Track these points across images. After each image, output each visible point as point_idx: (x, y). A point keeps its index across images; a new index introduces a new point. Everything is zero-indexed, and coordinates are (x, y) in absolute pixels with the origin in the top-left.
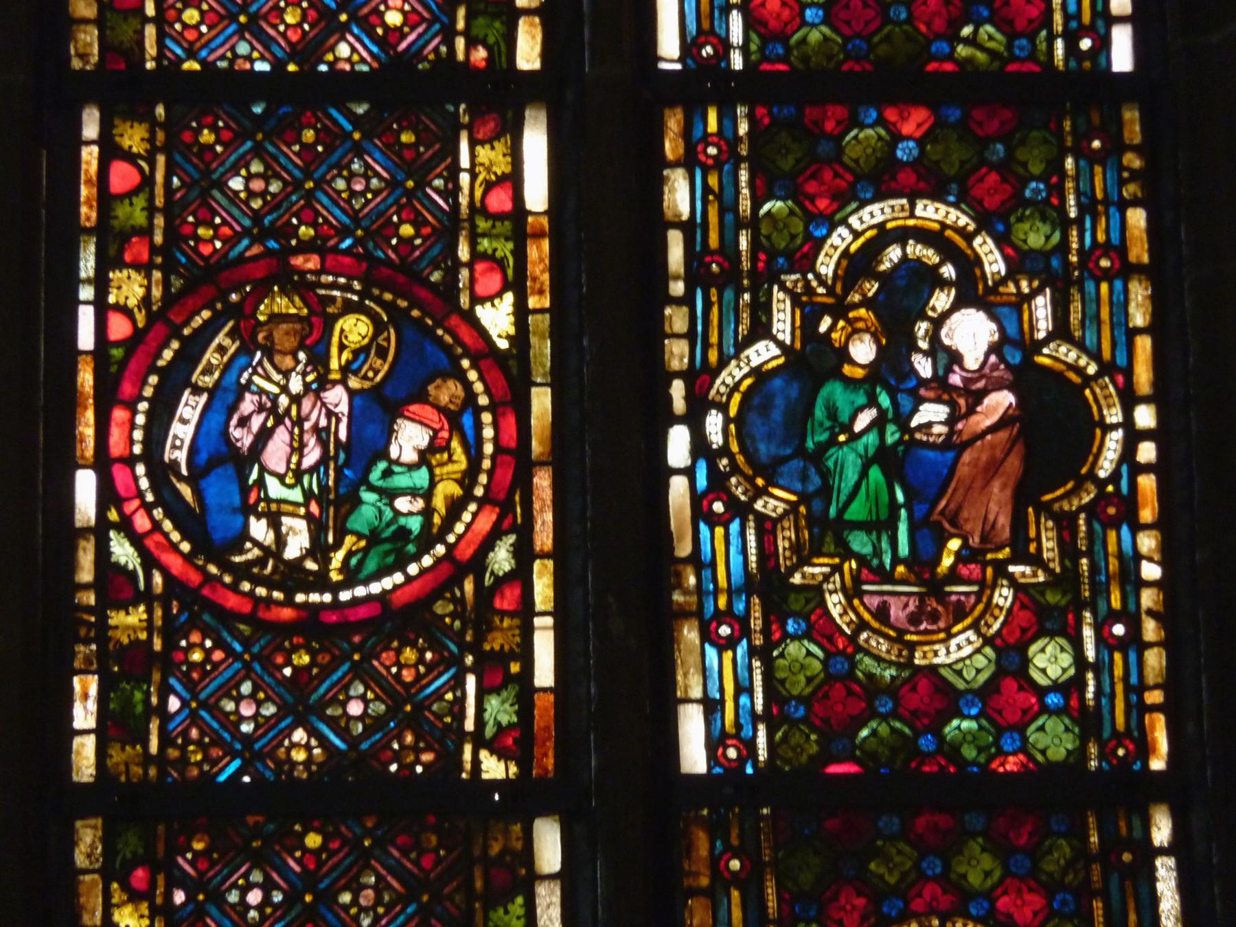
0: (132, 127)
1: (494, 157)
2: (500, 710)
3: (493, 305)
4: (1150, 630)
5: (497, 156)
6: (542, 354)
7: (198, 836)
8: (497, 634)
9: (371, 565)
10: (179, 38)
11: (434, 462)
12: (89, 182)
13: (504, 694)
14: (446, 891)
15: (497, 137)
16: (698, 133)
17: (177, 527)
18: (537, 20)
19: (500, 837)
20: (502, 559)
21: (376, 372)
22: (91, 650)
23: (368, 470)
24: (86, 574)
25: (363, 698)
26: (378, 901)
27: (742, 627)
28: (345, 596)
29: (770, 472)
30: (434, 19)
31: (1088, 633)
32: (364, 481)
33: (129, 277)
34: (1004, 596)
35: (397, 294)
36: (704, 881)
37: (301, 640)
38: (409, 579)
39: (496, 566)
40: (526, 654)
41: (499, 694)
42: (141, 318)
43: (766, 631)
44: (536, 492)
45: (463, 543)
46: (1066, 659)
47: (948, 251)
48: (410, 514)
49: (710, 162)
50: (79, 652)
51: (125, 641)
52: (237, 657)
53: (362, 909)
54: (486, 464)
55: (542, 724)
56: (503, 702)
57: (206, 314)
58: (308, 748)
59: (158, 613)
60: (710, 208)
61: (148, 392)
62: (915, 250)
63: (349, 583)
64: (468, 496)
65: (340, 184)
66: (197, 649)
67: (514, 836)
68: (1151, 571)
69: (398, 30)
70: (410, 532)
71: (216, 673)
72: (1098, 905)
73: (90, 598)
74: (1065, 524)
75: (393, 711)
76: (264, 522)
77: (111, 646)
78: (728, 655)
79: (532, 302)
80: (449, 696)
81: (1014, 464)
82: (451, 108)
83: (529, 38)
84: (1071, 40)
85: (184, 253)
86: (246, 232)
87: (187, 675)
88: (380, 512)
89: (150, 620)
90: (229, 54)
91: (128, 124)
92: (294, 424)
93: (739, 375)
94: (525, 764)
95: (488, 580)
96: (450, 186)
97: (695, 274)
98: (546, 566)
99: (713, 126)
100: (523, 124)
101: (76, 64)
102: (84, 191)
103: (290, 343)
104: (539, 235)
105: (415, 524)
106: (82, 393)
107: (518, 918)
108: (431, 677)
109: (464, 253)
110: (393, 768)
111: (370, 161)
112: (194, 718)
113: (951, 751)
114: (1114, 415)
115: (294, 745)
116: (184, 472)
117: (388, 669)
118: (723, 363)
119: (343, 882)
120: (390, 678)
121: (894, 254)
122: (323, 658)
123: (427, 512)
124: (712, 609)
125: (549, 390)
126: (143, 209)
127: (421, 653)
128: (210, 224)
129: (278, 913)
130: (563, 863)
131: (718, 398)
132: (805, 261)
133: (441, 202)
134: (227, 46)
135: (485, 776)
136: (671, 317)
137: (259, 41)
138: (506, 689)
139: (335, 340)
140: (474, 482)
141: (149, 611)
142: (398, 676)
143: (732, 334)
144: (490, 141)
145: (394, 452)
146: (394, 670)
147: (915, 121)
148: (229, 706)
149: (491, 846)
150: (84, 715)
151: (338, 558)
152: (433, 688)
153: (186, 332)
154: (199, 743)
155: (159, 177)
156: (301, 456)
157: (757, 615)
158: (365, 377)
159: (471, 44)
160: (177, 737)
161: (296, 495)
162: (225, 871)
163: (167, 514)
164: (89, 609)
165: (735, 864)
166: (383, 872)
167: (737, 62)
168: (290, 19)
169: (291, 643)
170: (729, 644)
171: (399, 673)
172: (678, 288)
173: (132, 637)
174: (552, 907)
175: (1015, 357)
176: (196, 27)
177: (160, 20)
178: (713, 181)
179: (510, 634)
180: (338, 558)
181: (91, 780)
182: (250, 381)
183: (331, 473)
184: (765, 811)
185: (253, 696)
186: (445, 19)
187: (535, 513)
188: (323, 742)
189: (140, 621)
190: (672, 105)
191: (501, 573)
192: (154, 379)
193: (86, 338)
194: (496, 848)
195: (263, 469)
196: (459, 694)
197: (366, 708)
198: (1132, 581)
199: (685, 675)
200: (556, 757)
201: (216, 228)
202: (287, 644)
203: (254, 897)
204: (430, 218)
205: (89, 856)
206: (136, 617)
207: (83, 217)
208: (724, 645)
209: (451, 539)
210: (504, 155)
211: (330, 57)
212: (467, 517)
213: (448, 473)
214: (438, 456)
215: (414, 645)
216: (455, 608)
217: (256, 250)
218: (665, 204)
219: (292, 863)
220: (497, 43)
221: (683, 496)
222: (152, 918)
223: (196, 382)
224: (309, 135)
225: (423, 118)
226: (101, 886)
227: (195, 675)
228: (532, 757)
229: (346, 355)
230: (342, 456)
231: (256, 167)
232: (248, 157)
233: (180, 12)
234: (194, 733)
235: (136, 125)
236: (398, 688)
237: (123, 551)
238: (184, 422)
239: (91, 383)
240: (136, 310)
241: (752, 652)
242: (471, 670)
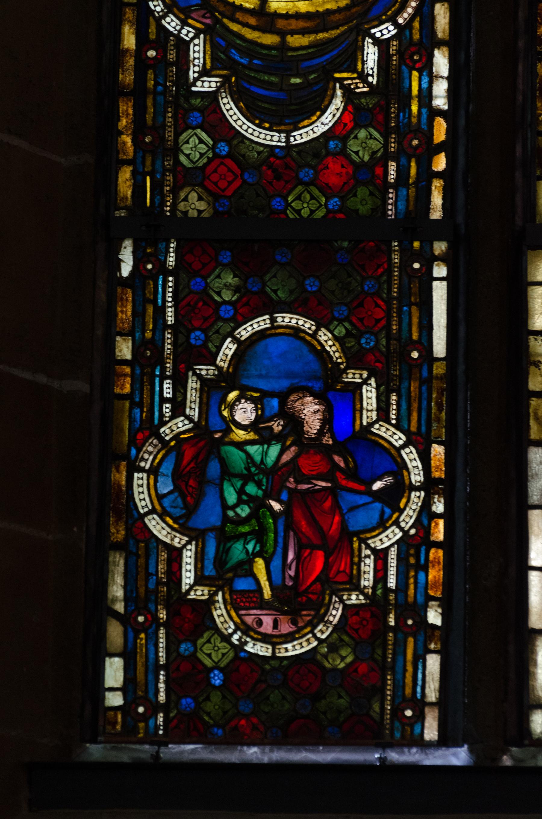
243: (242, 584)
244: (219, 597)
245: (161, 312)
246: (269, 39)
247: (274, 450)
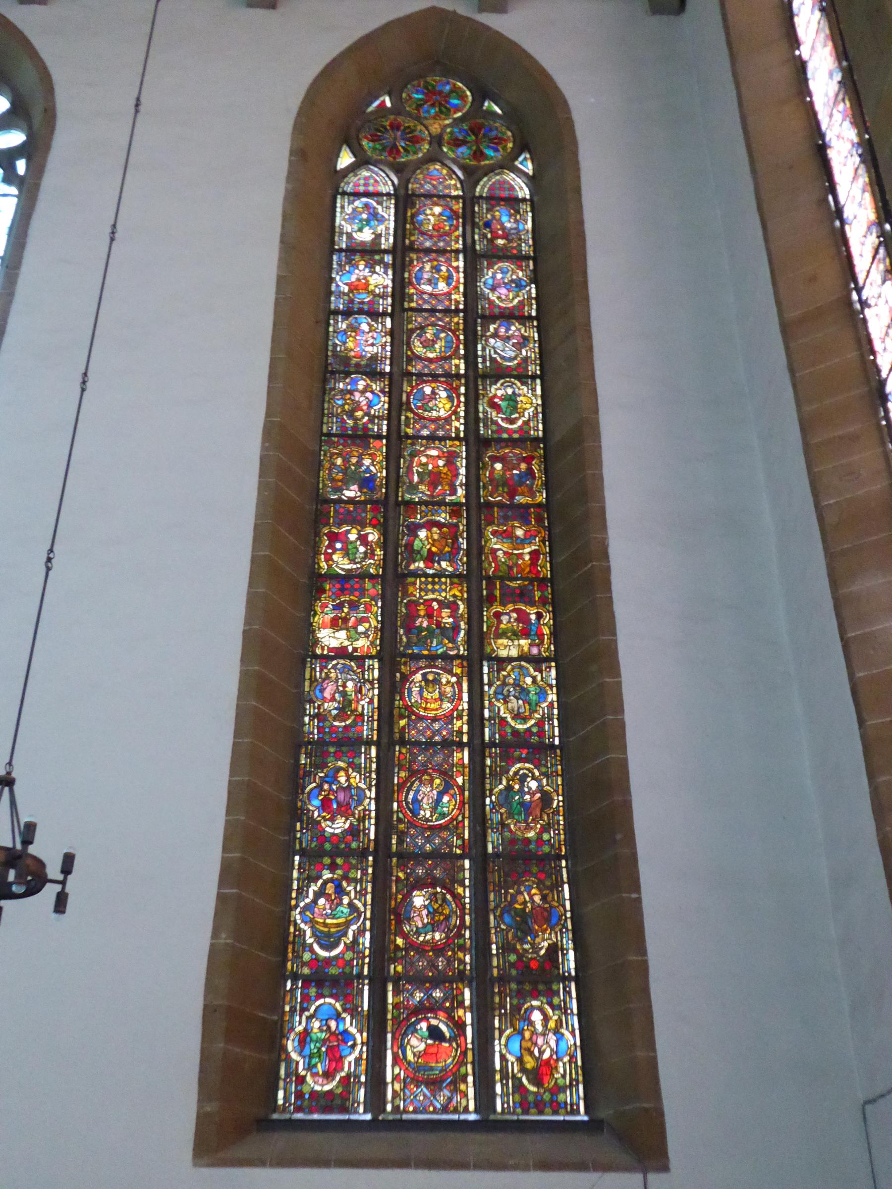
1: (460, 755)
2: (460, 842)
4: (562, 832)
20: (460, 818)
27: (498, 829)
29: (501, 806)
31: (552, 832)
34: (539, 826)
40: (464, 834)
46: (548, 836)
47: (530, 772)
62: (525, 771)
68: (562, 823)
72: (554, 876)
73: (395, 823)
74: (548, 815)
75: (443, 842)
81: (541, 805)
84: (549, 739)
94: (463, 851)
97: (490, 774)
105: (447, 812)
109: (455, 770)
113: (530, 851)
114: (556, 798)
121: (521, 772)
132: (507, 772)
147: (526, 751)
150: (394, 841)
151: (434, 817)
167: (497, 741)
168: (429, 733)
170: (495, 833)
172: (488, 776)
175: (540, 788)
177: (408, 733)
180: (434, 817)
198: (559, 824)
203: (420, 871)
206: (403, 826)
237: (401, 815)
243: (314, 1070)
244: (309, 1074)
245: (296, 998)
246: (326, 930)
247: (324, 1034)
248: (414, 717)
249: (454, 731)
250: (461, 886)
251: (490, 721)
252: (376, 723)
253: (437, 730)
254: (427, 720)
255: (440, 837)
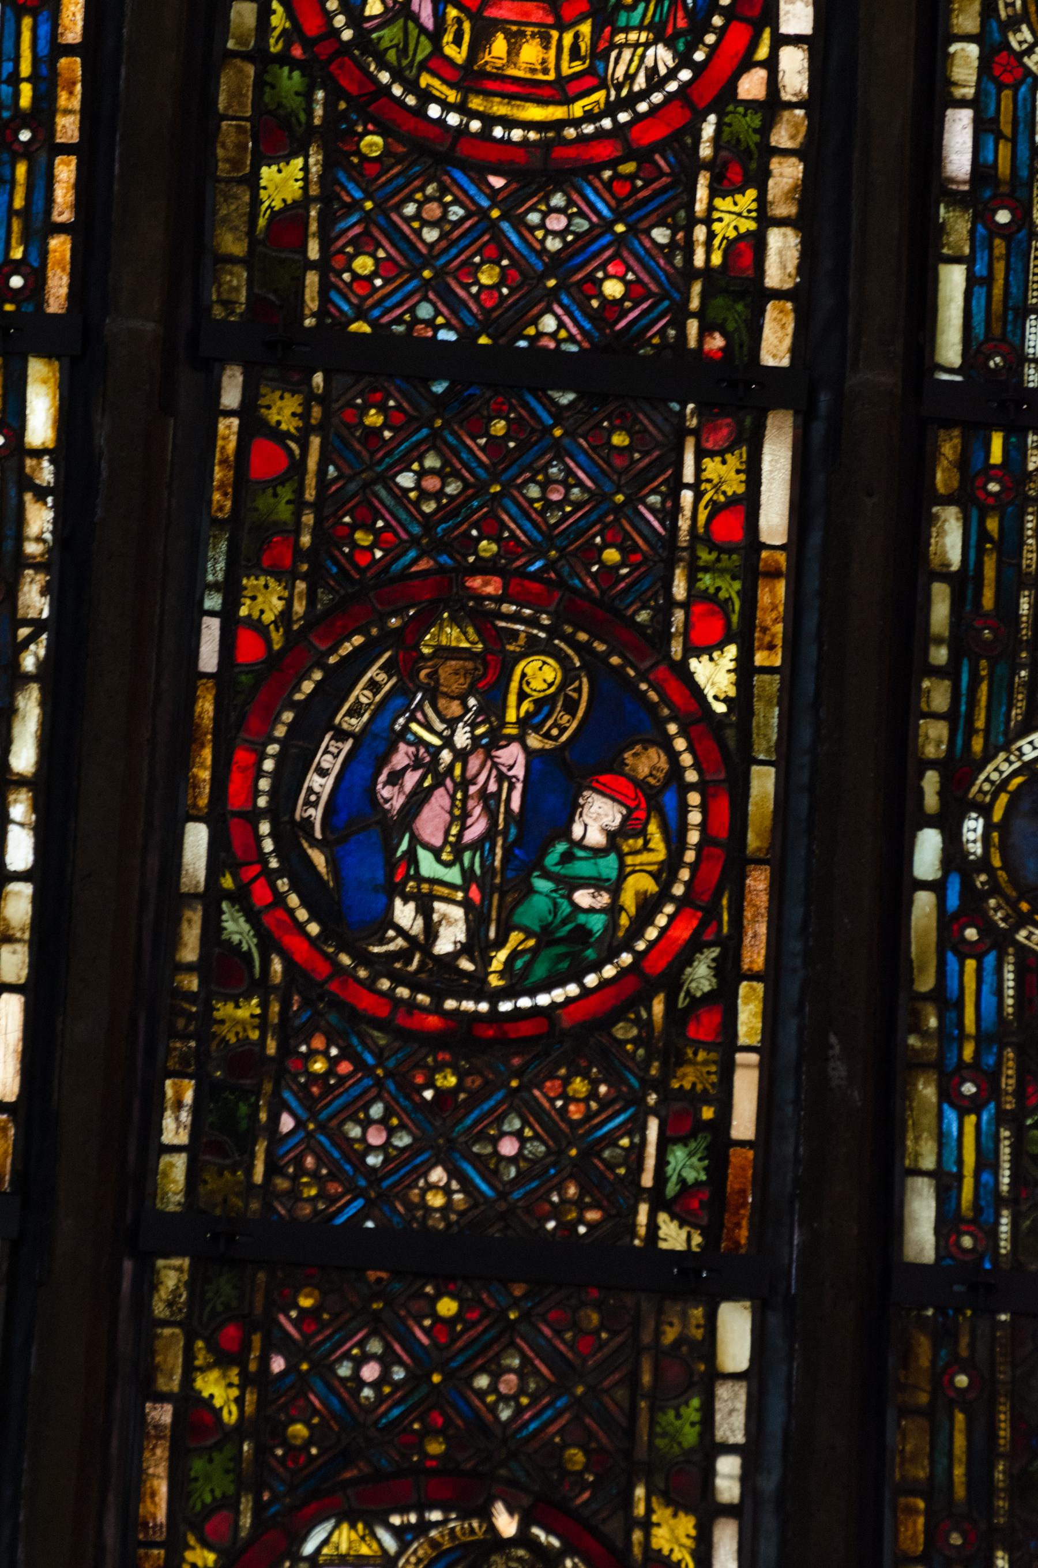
0: (282, 398)
3: (711, 659)
5: (728, 472)
6: (767, 725)
7: (307, 1290)
8: (689, 1069)
9: (540, 971)
10: (346, 290)
11: (626, 849)
12: (224, 462)
13: (693, 1145)
14: (607, 1383)
15: (730, 450)
16: (978, 464)
17: (304, 903)
18: (789, 305)
19: (676, 1321)
21: (563, 730)
22: (190, 1048)
23: (544, 853)
24: (190, 953)
25: (518, 1134)
26: (522, 1391)
28: (505, 1006)
30: (664, 296)
32: (537, 865)
33: (266, 586)
35: (594, 636)
36: (924, 1398)
37: (447, 1057)
38: (585, 991)
39: (694, 985)
41: (686, 1145)
42: (277, 639)
43: (1020, 1093)
44: (748, 897)
45: (654, 953)
48: (591, 910)
49: (991, 501)
50: (175, 1049)
51: (233, 1040)
52: (369, 1071)
53: (503, 1398)
54: (690, 856)
55: (736, 1186)
56: (690, 1155)
57: (358, 640)
58: (447, 1191)
59: (275, 1008)
60: (986, 559)
61: (280, 732)
63: (510, 992)
64: (664, 895)
65: (534, 491)
66: (320, 1057)
67: (694, 1322)
69: (619, 302)
70: (590, 933)
71: (342, 1090)
73: (192, 983)
75: (556, 1154)
76: (412, 905)
77: (214, 1046)
78: (971, 1120)
79: (760, 658)
80: (625, 1142)
82: (675, 406)
83: (778, 328)
85: (336, 563)
86: (415, 541)
87: (305, 1087)
88: (555, 904)
89: (263, 1017)
90: (407, 317)
91: (278, 393)
92: (457, 786)
93: (1007, 769)
94: (711, 1235)
95: (682, 1002)
96: (669, 504)
98: (754, 990)
99: (996, 455)
100: (764, 436)
101: (218, 312)
102: (218, 474)
103: (458, 685)
104: (775, 574)
105: (597, 923)
106: (199, 726)
107: (693, 1424)
108: (603, 1116)
109: (680, 590)
110: (551, 1225)
111: (572, 464)
112: (310, 1144)
115: (431, 1187)
116: (318, 835)
117: (552, 1101)
118: (988, 757)
119: (479, 1362)
120: (553, 1113)
122: (473, 1082)
123: (614, 910)
124: (955, 1060)
125: (772, 770)
126: (288, 502)
127: (594, 1084)
128: (370, 528)
129: (399, 1395)
130: (752, 1360)
131: (980, 798)
133: (656, 524)
134: (405, 307)
135: (663, 1245)
136: (929, 692)
137: (446, 304)
138: (696, 1140)
139: (514, 686)
140: (673, 878)
141: (264, 1005)
142: (563, 1111)
143: (1002, 718)
144: (721, 453)
145: (577, 831)
146: (559, 1103)
148: (355, 1132)
149: (664, 1333)
152: (606, 1129)
153: (332, 660)
154: (315, 1175)
155: (312, 463)
156: (463, 828)
157: (1010, 1072)
158: (547, 736)
159: (704, 331)
160: (287, 1165)
161: (454, 875)
162: (337, 1337)
163: (294, 887)
164: (191, 997)
165: (962, 1380)
166: (531, 1354)
168: (487, 277)
169: (435, 1060)
170: (974, 1105)
171: (565, 1107)
172: (940, 655)
173: (241, 1036)
174: (734, 1414)
176: (369, 278)
177: (323, 266)
178: (992, 525)
179: (705, 1069)
181: (178, 1209)
182: (406, 728)
183: (499, 851)
184: (1003, 1317)
185: (384, 1121)
186: (676, 295)
187: (745, 922)
188: (467, 1185)
189: (252, 1016)
190: (948, 424)
191: (699, 994)
192: (288, 716)
193: (209, 658)
194: (670, 1335)
195: (416, 841)
196: (637, 1140)
197: (522, 1148)
199: (917, 1139)
200: (750, 1230)
201: (377, 533)
202: (430, 1060)
203: (370, 1372)
204: (640, 542)
205: (170, 1304)
207: (215, 506)
208: (965, 1107)
209: (641, 946)
210: (738, 472)
211: (531, 331)
212: (661, 920)
213: (641, 864)
214: (631, 841)
215: (586, 1076)
216: (640, 1032)
217: (424, 565)
218: (932, 548)
219: (419, 1334)
220: (737, 329)
221: (928, 916)
222: (242, 1387)
223: (340, 724)
224: (499, 427)
225: (641, 416)
226: (182, 1343)
227: (315, 1090)
228: (722, 1226)
229: (526, 706)
230: (513, 831)
231: (431, 461)
232: (423, 448)
233: (353, 257)
234: (310, 1161)
235: (287, 395)
236: (563, 1125)
238: (323, 773)
239: (211, 714)
240: (272, 627)
241: (1001, 1118)
242: (654, 1111)
248: (373, 143)
249: (690, 273)
250: (678, 1505)
251: (982, 216)
252: (65, 171)
253: (556, 262)
254: (479, 173)
255: (531, 1112)
